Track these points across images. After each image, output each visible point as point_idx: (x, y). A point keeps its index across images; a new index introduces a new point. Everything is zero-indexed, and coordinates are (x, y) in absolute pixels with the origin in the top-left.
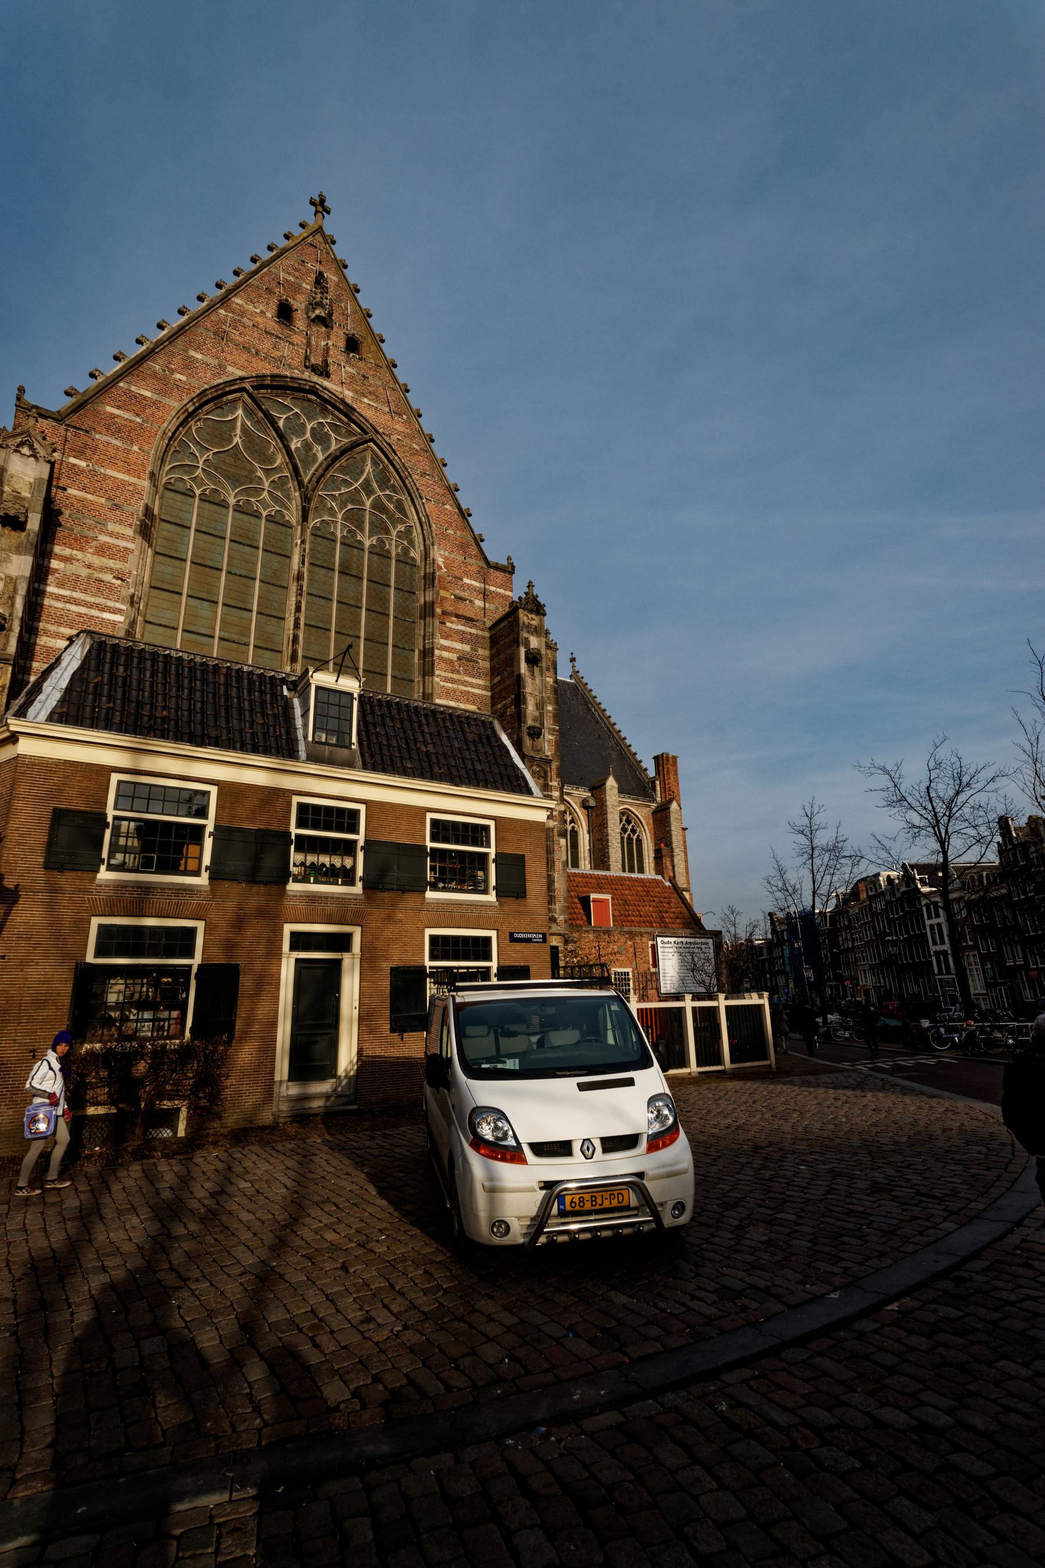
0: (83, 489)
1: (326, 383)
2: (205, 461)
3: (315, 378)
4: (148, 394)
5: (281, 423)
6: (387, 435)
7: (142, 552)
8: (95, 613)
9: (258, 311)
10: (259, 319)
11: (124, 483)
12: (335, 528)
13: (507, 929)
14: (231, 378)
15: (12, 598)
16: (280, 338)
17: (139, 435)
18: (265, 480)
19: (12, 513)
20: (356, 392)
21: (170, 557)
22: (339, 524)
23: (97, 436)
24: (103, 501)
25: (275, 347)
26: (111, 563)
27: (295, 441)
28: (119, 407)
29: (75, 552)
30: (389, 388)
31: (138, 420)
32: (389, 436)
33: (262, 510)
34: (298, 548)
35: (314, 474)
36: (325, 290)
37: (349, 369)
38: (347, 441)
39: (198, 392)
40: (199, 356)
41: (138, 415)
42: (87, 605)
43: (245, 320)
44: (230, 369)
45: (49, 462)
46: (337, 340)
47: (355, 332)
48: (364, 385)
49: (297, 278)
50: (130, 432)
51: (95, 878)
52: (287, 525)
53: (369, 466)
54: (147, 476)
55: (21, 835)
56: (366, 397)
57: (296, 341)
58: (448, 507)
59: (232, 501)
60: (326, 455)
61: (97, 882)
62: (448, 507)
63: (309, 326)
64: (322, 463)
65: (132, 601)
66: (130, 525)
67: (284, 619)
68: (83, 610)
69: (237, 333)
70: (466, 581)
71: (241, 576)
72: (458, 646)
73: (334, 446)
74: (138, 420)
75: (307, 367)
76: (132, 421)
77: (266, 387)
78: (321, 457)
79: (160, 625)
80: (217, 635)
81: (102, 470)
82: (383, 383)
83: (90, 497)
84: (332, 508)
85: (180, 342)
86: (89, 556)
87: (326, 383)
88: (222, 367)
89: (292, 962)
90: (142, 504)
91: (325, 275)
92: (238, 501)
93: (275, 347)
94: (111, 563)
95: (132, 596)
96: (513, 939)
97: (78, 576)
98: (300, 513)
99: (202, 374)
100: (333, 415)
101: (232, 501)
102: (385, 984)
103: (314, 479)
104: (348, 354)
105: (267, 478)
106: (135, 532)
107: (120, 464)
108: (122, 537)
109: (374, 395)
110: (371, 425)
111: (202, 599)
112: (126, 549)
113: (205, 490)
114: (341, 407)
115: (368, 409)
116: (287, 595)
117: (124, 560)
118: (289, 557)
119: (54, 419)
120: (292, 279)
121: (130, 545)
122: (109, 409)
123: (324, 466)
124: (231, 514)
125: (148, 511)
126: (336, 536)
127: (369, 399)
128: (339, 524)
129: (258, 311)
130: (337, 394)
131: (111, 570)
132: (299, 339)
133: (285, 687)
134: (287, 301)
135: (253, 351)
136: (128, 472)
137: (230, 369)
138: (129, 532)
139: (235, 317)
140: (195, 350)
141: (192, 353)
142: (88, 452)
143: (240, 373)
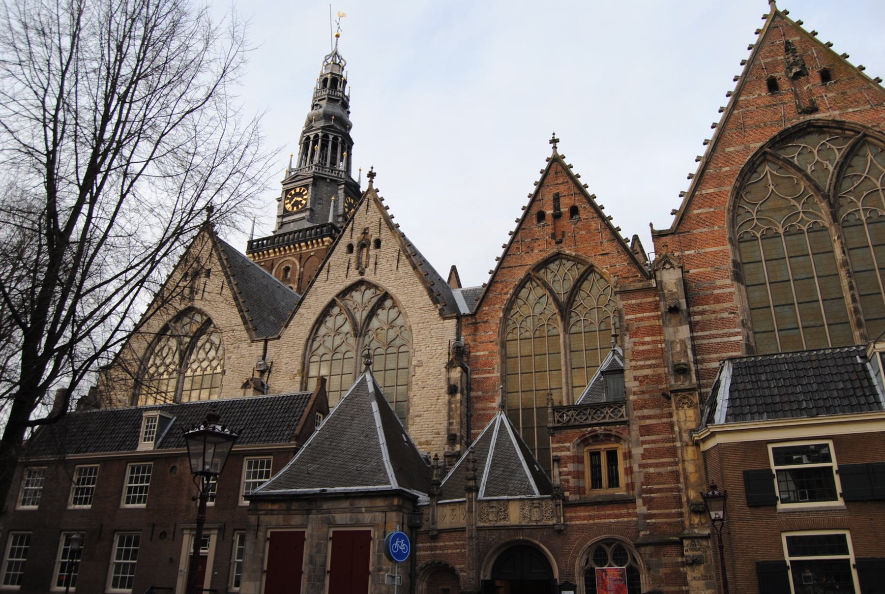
0: (697, 267)
1: (817, 116)
2: (757, 212)
3: (809, 117)
4: (711, 191)
5: (795, 160)
6: (875, 126)
7: (740, 290)
8: (725, 339)
9: (756, 96)
10: (759, 101)
11: (717, 252)
12: (860, 215)
14: (755, 152)
15: (686, 352)
16: (776, 105)
17: (715, 219)
18: (798, 205)
19: (672, 306)
20: (840, 108)
21: (755, 285)
22: (861, 211)
23: (695, 232)
24: (709, 269)
25: (775, 113)
26: (725, 305)
27: (809, 167)
28: (700, 208)
29: (704, 307)
30: (865, 89)
31: (712, 210)
32: (878, 126)
33: (803, 227)
34: (837, 242)
35: (830, 184)
36: (794, 51)
37: (830, 95)
38: (846, 146)
39: (739, 172)
40: (732, 149)
41: (711, 207)
42: (721, 336)
43: (751, 108)
44: (752, 146)
45: (680, 267)
46: (815, 77)
47: (825, 66)
48: (845, 99)
49: (773, 57)
50: (710, 219)
51: (776, 509)
52: (824, 229)
53: (870, 155)
54: (727, 242)
55: (731, 489)
56: (849, 107)
57: (786, 100)
59: (781, 231)
60: (834, 165)
61: (778, 511)
63: (792, 83)
64: (833, 173)
65: (743, 324)
66: (728, 277)
67: (843, 298)
68: (719, 340)
69: (749, 119)
71: (803, 279)
73: (838, 156)
74: (712, 210)
75: (800, 113)
76: (709, 213)
77: (778, 142)
78: (831, 168)
79: (764, 332)
80: (800, 326)
81: (703, 251)
82: (859, 89)
83: (702, 270)
84: (852, 201)
85: (719, 147)
86: (712, 306)
87: (817, 116)
88: (747, 148)
90: (730, 260)
91: (790, 41)
92: (786, 229)
93: (775, 113)
95: (742, 321)
97: (710, 320)
98: (830, 217)
99: (737, 160)
100: (829, 132)
101: (781, 231)
103: (832, 188)
104: (826, 84)
105: (799, 203)
106: (732, 280)
107: (711, 242)
109: (856, 102)
110: (861, 125)
111: (784, 305)
112: (730, 293)
113: (763, 232)
114: (834, 125)
115: (854, 115)
116: (839, 281)
117: (731, 300)
118: (832, 252)
119: (672, 234)
120: (770, 60)
121: (732, 290)
122: (695, 212)
123: (835, 175)
124: (783, 240)
125: (735, 263)
126: (862, 221)
127: (853, 108)
128: (861, 211)
129: (756, 96)
130: (827, 118)
131: (726, 309)
132: (788, 98)
133: (858, 357)
134: (772, 76)
135: (762, 124)
136: (716, 245)
137: (752, 146)
139: (744, 110)
140: (729, 147)
141: (728, 150)
142: (693, 244)
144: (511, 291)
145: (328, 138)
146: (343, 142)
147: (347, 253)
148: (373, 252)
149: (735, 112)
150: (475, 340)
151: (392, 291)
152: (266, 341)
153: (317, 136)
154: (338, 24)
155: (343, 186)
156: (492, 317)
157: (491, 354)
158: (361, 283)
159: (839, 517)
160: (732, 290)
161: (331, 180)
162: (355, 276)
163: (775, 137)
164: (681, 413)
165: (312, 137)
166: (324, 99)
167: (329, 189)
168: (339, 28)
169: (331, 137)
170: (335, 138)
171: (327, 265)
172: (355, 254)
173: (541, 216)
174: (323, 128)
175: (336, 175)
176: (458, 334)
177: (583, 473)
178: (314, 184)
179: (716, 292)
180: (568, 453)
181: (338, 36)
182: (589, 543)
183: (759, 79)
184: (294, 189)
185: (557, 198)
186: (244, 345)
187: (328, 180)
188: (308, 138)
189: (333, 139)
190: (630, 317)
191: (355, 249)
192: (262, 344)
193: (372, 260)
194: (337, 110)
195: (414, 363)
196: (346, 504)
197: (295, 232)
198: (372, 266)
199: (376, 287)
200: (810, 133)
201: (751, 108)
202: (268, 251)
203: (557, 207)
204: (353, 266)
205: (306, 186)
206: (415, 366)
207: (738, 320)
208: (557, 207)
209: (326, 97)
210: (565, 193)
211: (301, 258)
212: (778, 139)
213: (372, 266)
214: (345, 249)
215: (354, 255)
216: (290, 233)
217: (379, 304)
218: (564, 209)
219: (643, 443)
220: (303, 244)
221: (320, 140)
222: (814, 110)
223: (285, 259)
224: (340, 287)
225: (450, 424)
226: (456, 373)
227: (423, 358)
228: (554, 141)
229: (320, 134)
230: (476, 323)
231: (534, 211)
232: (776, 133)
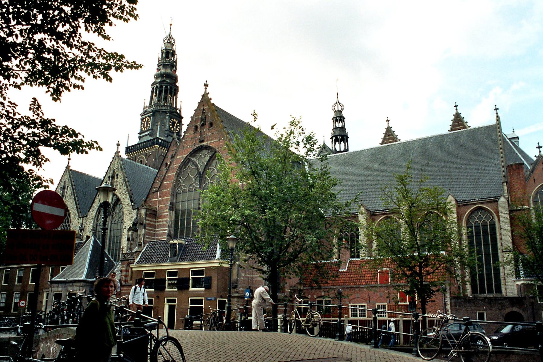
1: (204, 143)
4: (170, 174)
43: (188, 139)
65: (169, 226)
94: (165, 219)
108: (167, 212)
121: (168, 213)
122: (165, 183)
138: (167, 210)
143: (185, 156)
145: (163, 87)
146: (171, 88)
151: (120, 197)
152: (83, 217)
153: (157, 86)
155: (168, 114)
159: (153, 293)
160: (168, 213)
161: (162, 112)
165: (155, 88)
167: (162, 116)
169: (164, 87)
170: (166, 87)
174: (159, 82)
175: (167, 108)
178: (153, 115)
180: (124, 269)
181: (171, 25)
183: (192, 126)
184: (145, 118)
186: (76, 219)
189: (165, 88)
192: (82, 218)
193: (115, 184)
195: (124, 227)
196: (71, 284)
199: (117, 196)
200: (203, 149)
201: (188, 139)
205: (150, 117)
207: (167, 225)
211: (146, 156)
212: (192, 153)
214: (108, 179)
220: (147, 149)
222: (203, 141)
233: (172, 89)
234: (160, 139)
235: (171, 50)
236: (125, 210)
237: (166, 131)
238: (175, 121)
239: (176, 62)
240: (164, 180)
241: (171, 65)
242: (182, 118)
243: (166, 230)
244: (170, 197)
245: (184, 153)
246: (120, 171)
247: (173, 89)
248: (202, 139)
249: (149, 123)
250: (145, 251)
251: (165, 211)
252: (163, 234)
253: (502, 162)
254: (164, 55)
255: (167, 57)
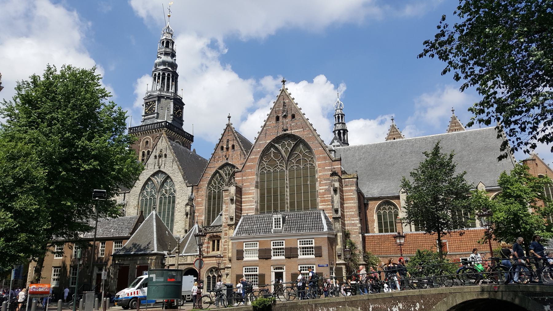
1: (287, 132)
4: (253, 157)
8: (250, 207)
11: (252, 178)
13: (317, 264)
58: (320, 149)
62: (320, 149)
68: (248, 207)
70: (326, 168)
72: (324, 187)
73: (293, 145)
87: (287, 132)
89: (274, 273)
96: (319, 266)
102: (290, 277)
121: (254, 191)
136: (252, 176)
138: (254, 188)
141: (260, 142)
143: (269, 141)
144: (210, 177)
145: (165, 74)
146: (173, 76)
147: (155, 159)
148: (164, 159)
149: (265, 128)
150: (197, 195)
151: (170, 175)
152: (125, 193)
153: (159, 74)
154: (169, 9)
156: (204, 186)
157: (202, 200)
158: (159, 172)
160: (254, 191)
161: (166, 97)
162: (157, 169)
163: (274, 139)
164: (230, 231)
165: (157, 74)
166: (163, 53)
168: (170, 11)
169: (166, 74)
170: (168, 75)
171: (147, 163)
172: (157, 160)
173: (222, 148)
174: (162, 70)
176: (192, 192)
177: (210, 247)
179: (250, 191)
181: (169, 16)
182: (208, 268)
183: (273, 116)
184: (149, 102)
185: (228, 142)
187: (165, 97)
188: (155, 75)
190: (226, 198)
191: (157, 157)
192: (123, 194)
193: (163, 162)
194: (169, 59)
197: (150, 124)
198: (163, 165)
202: (138, 133)
203: (227, 145)
204: (157, 164)
206: (177, 204)
208: (227, 145)
209: (163, 52)
210: (231, 139)
213: (163, 165)
215: (157, 160)
216: (148, 125)
217: (165, 181)
218: (230, 146)
219: (225, 238)
221: (161, 76)
223: (146, 137)
224: (152, 173)
225: (186, 226)
226: (188, 208)
227: (180, 201)
228: (229, 117)
229: (161, 73)
230: (198, 188)
231: (220, 146)
232: (275, 138)
233: (174, 77)
234: (168, 123)
235: (171, 40)
236: (177, 187)
237: (171, 115)
238: (178, 107)
239: (175, 52)
240: (247, 162)
241: (172, 55)
242: (184, 105)
243: (253, 205)
244: (255, 177)
245: (267, 139)
246: (168, 151)
247: (175, 77)
248: (285, 128)
249: (154, 107)
250: (241, 224)
251: (251, 188)
252: (250, 209)
253: (514, 158)
254: (165, 45)
255: (167, 46)
